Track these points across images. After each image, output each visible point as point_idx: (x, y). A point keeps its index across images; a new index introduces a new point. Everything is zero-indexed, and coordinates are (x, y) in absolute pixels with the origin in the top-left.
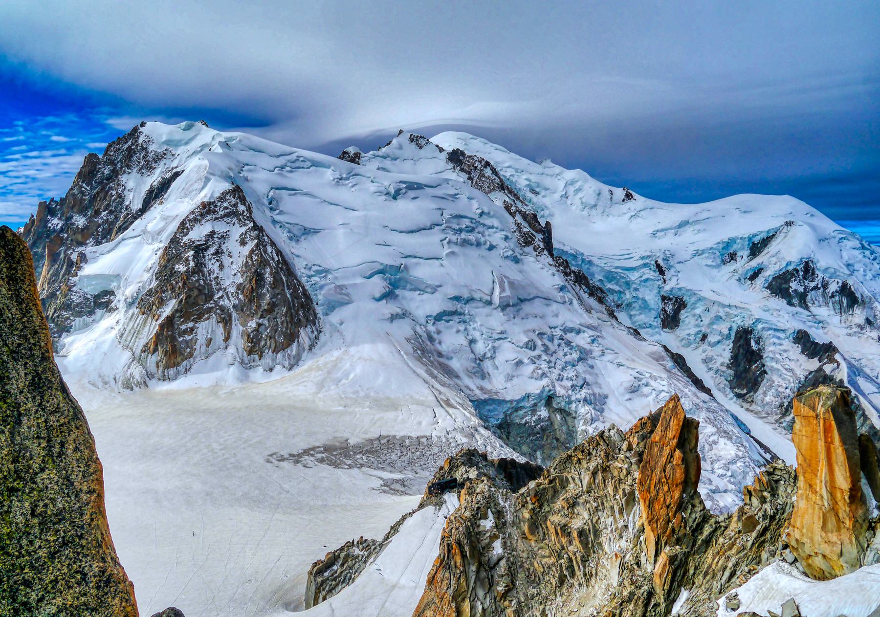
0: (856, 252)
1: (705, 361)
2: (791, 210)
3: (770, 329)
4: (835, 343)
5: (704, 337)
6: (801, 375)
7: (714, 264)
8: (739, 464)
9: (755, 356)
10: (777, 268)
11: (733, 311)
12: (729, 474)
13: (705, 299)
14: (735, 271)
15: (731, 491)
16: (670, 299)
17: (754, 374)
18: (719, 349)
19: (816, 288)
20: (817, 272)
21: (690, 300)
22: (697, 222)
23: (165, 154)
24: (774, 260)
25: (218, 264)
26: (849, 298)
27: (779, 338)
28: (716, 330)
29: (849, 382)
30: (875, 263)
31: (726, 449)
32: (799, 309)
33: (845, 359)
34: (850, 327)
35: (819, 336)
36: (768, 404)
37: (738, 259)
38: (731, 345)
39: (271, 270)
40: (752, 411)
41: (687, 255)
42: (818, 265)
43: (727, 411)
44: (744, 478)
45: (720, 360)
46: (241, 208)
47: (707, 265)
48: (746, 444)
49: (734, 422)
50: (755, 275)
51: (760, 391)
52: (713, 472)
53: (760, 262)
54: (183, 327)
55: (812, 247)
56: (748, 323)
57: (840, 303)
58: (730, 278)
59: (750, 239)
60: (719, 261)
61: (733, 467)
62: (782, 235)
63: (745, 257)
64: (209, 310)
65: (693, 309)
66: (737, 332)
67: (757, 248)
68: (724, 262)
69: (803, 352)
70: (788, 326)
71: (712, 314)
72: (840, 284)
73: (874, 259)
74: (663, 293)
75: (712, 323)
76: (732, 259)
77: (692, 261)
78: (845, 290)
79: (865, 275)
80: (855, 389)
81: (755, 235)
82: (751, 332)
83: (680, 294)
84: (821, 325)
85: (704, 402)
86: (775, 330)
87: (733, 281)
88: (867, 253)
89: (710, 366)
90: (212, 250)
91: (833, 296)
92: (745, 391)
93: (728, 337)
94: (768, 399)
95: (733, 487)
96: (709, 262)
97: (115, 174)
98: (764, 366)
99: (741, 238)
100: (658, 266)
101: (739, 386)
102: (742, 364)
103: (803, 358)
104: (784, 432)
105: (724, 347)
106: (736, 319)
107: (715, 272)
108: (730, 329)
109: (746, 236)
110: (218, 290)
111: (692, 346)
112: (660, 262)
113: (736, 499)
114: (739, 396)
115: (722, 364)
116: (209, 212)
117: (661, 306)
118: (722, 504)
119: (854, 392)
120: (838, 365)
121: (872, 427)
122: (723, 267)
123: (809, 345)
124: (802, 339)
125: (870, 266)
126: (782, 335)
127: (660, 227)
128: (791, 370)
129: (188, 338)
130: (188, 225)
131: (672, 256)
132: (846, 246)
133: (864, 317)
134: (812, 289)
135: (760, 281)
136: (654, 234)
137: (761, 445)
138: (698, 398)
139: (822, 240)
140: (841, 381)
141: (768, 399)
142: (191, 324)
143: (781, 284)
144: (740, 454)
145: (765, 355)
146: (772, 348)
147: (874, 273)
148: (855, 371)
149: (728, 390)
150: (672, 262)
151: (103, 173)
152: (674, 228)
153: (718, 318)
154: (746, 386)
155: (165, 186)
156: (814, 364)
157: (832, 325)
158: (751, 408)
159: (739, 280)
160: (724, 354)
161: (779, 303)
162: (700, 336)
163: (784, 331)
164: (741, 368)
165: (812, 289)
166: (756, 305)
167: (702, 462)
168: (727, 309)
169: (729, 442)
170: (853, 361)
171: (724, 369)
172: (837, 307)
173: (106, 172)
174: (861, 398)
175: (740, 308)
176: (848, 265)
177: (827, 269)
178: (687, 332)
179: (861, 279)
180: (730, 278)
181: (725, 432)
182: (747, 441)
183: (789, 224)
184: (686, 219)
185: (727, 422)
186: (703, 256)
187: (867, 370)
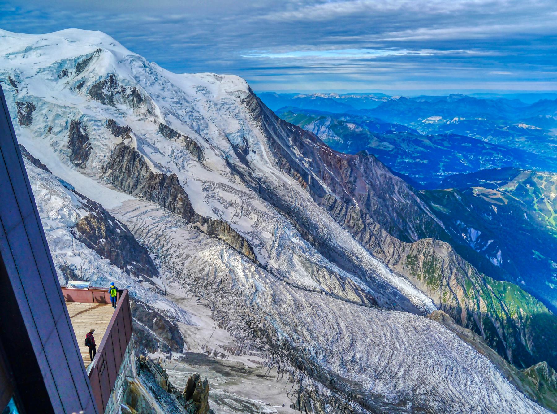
0: (141, 69)
1: (52, 145)
2: (101, 41)
3: (91, 120)
4: (131, 126)
5: (50, 129)
6: (112, 147)
7: (53, 78)
8: (65, 210)
9: (84, 139)
10: (94, 80)
11: (68, 110)
12: (60, 217)
13: (48, 103)
14: (68, 83)
15: (61, 227)
16: (23, 104)
17: (85, 150)
18: (60, 136)
19: (118, 92)
20: (118, 82)
21: (38, 105)
22: (39, 48)
24: (92, 75)
26: (137, 98)
27: (98, 126)
28: (57, 124)
29: (138, 149)
30: (152, 76)
31: (57, 202)
32: (109, 106)
33: (135, 135)
34: (139, 115)
35: (122, 123)
36: (94, 167)
37: (69, 74)
38: (69, 133)
40: (85, 174)
41: (33, 72)
42: (119, 78)
43: (56, 178)
44: (70, 218)
45: (62, 143)
47: (48, 79)
48: (69, 196)
49: (60, 184)
50: (81, 86)
51: (89, 160)
52: (49, 218)
53: (83, 76)
55: (114, 66)
56: (77, 118)
57: (133, 101)
58: (65, 88)
59: (75, 61)
60: (56, 76)
61: (63, 212)
62: (96, 58)
63: (74, 73)
65: (41, 110)
66: (72, 124)
67: (81, 66)
68: (60, 77)
69: (112, 133)
70: (103, 117)
71: (54, 113)
72: (132, 90)
73: (151, 73)
74: (17, 101)
75: (54, 120)
76: (65, 75)
77: (37, 76)
78: (134, 93)
79: (146, 84)
80: (142, 153)
81: (79, 58)
82: (80, 123)
83: (30, 100)
84: (123, 115)
85: (39, 174)
86: (95, 121)
87: (67, 90)
88: (147, 69)
89: (56, 148)
91: (128, 97)
92: (80, 162)
93: (66, 127)
94: (94, 165)
95: (62, 224)
96: (49, 77)
98: (90, 144)
99: (70, 60)
100: (11, 81)
101: (76, 159)
102: (77, 145)
103: (113, 137)
104: (105, 183)
105: (64, 134)
106: (70, 115)
107: (54, 83)
108: (67, 122)
109: (73, 58)
111: (44, 136)
112: (12, 77)
113: (64, 231)
114: (77, 165)
115: (64, 146)
117: (18, 109)
118: (55, 237)
119: (141, 154)
120: (132, 139)
121: (151, 173)
122: (60, 80)
123: (115, 128)
124: (111, 125)
125: (149, 77)
126: (99, 124)
127: (11, 51)
128: (106, 145)
131: (22, 73)
132: (134, 65)
133: (146, 109)
134: (116, 93)
135: (84, 89)
136: (7, 56)
137: (80, 195)
138: (34, 172)
139: (120, 61)
140: (134, 148)
141: (94, 165)
143: (97, 91)
144: (66, 203)
145: (90, 138)
146: (94, 132)
147: (151, 82)
148: (142, 141)
149: (69, 162)
150: (21, 77)
152: (22, 52)
153: (58, 115)
154: (80, 158)
156: (119, 140)
157: (130, 117)
158: (85, 172)
159: (71, 89)
160: (64, 139)
161: (96, 103)
162: (48, 128)
163: (100, 121)
164: (76, 147)
165: (116, 93)
166: (83, 105)
167: (40, 214)
168: (63, 109)
169: (58, 198)
170: (141, 136)
171: (65, 149)
172: (131, 103)
174: (145, 157)
175: (72, 108)
176: (136, 78)
177: (124, 80)
178: (38, 126)
179: (144, 86)
180: (65, 88)
181: (54, 191)
182: (69, 195)
183: (99, 51)
184: (30, 45)
185: (55, 185)
186: (45, 73)
187: (148, 140)
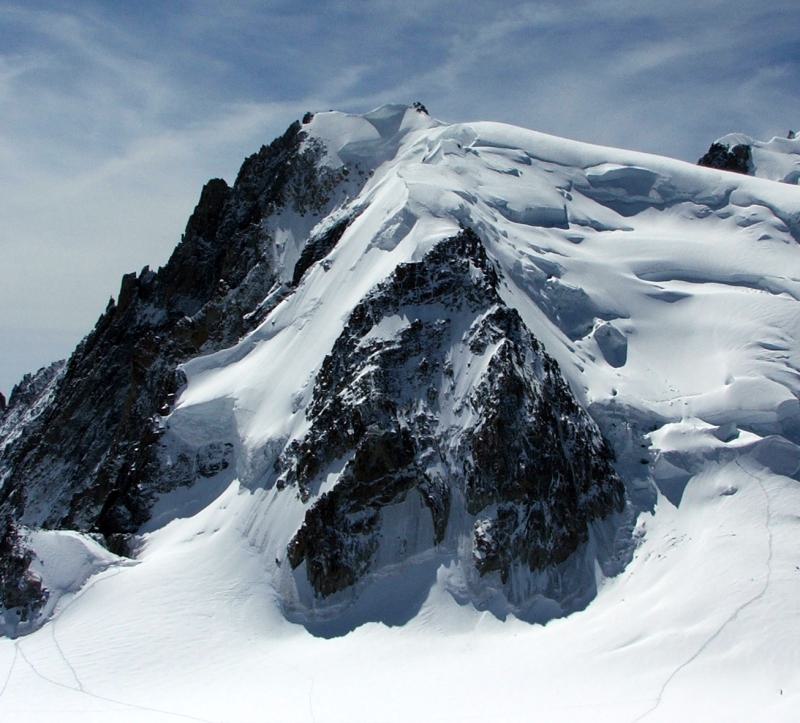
23: (346, 173)
54: (353, 518)
97: (256, 214)
110: (425, 444)
129: (363, 538)
130: (369, 313)
151: (234, 216)
155: (334, 235)
173: (240, 213)
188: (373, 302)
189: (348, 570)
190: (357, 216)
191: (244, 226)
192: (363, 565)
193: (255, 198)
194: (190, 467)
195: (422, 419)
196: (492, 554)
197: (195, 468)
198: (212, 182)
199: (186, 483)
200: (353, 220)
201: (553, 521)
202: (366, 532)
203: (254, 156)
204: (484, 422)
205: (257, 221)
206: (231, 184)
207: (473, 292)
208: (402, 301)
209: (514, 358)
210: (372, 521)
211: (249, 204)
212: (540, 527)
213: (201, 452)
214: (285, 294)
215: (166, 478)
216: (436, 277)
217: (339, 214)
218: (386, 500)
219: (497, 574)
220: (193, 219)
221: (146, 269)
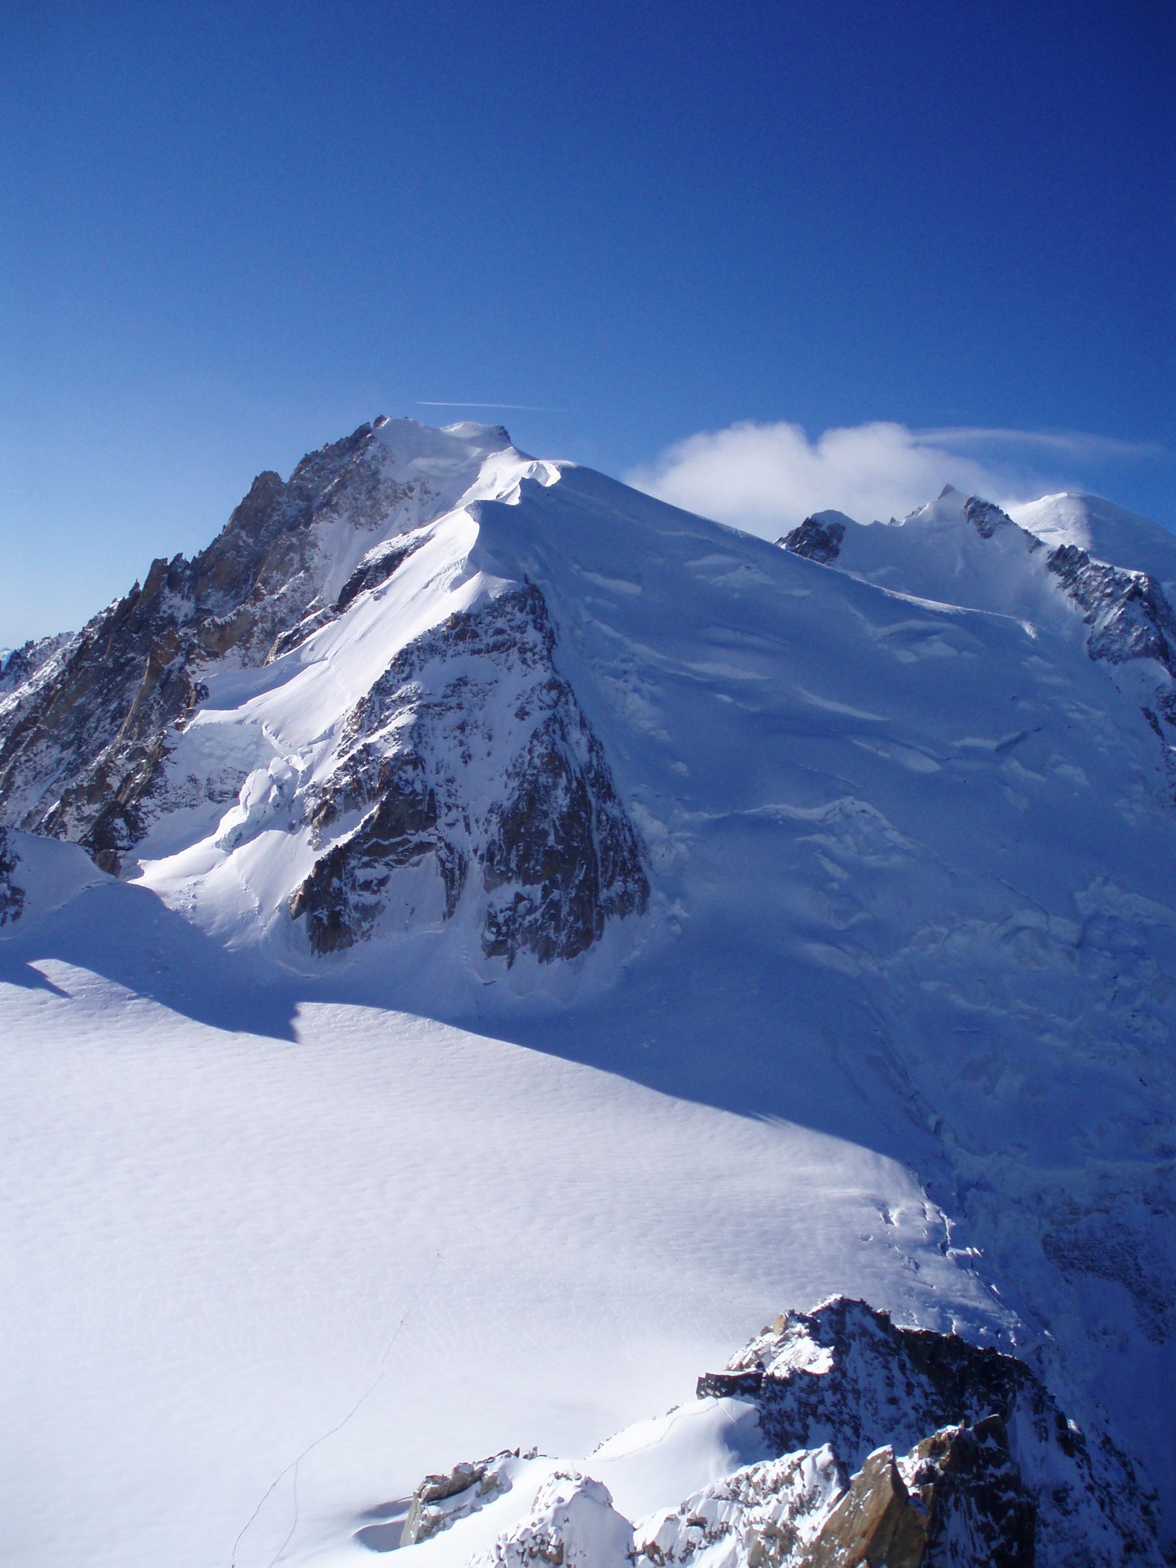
25: (460, 750)
39: (570, 781)
46: (532, 636)
54: (362, 875)
64: (423, 847)
90: (453, 718)
116: (461, 636)
129: (369, 898)
130: (414, 657)
142: (379, 871)
155: (391, 562)
173: (291, 512)
188: (419, 649)
189: (348, 930)
190: (417, 548)
191: (292, 528)
192: (365, 926)
193: (309, 498)
194: (198, 790)
195: (451, 781)
196: (501, 938)
197: (202, 793)
198: (265, 474)
199: (192, 806)
200: (413, 551)
201: (569, 914)
202: (375, 892)
203: (315, 454)
204: (516, 797)
205: (307, 525)
206: (285, 479)
207: (529, 655)
208: (450, 652)
209: (559, 733)
210: (382, 882)
211: (302, 504)
212: (555, 917)
213: (214, 777)
214: (327, 618)
215: (171, 797)
216: (490, 632)
217: (399, 541)
218: (400, 862)
219: (501, 960)
220: (238, 510)
221: (180, 555)
